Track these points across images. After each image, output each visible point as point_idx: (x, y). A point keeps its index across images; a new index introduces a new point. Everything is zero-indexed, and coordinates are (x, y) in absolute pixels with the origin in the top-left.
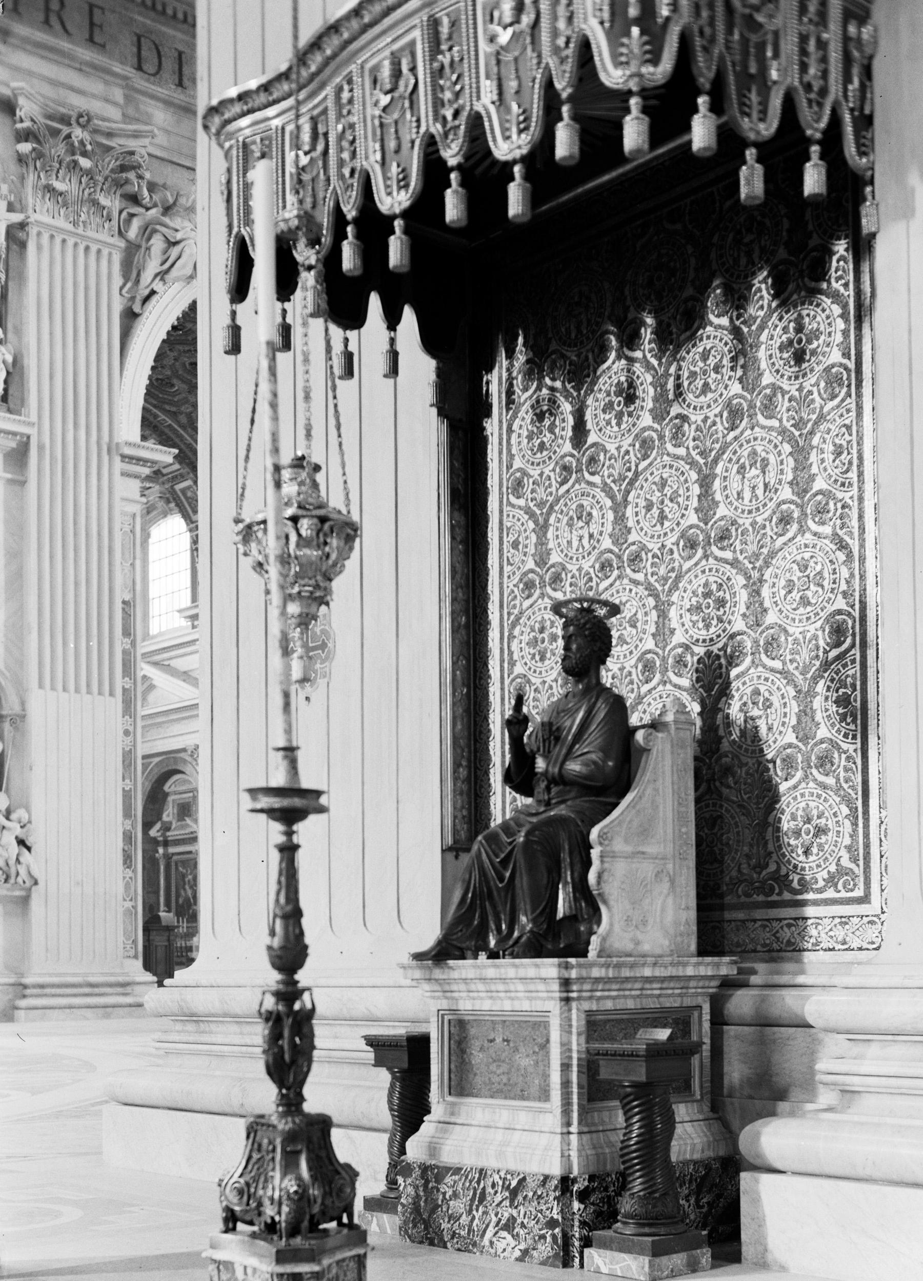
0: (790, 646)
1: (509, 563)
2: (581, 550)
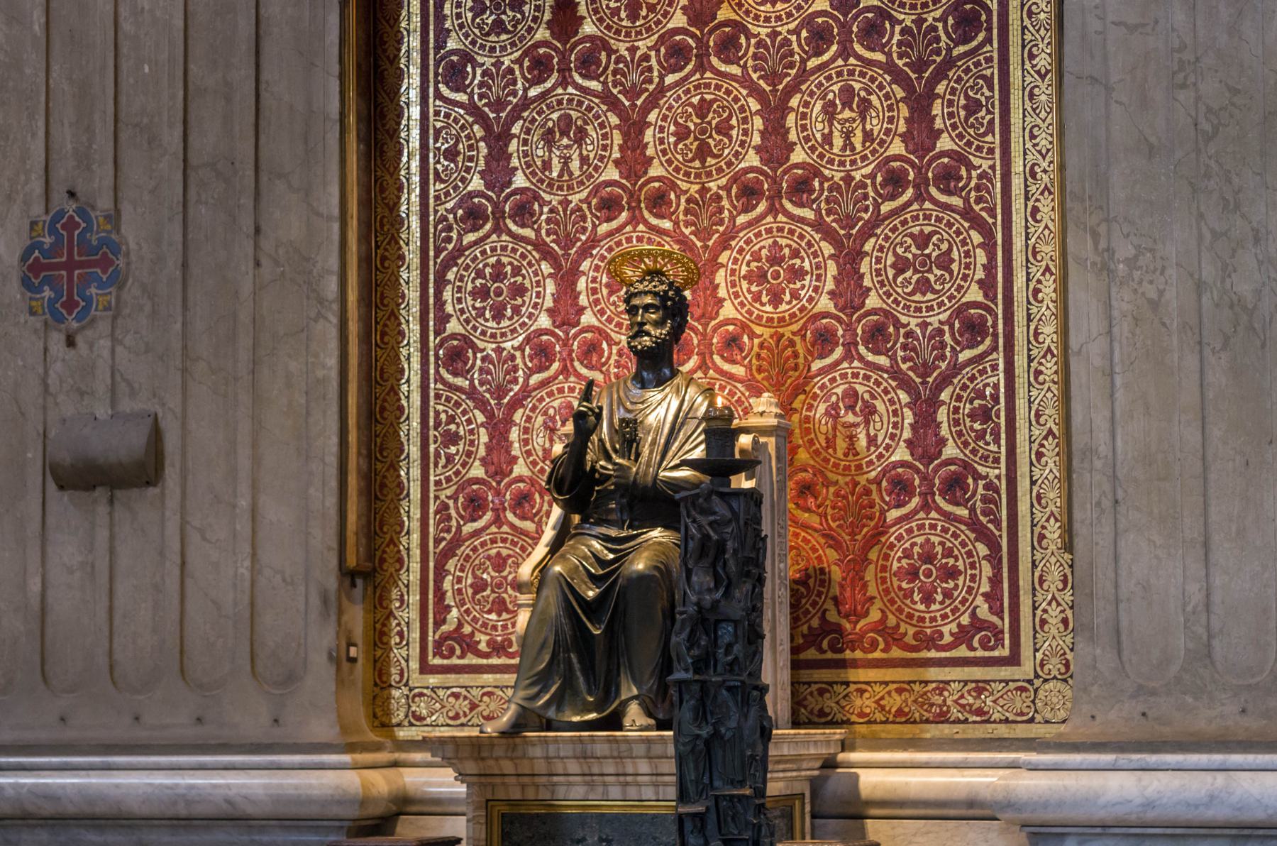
0: (902, 340)
2: (566, 177)
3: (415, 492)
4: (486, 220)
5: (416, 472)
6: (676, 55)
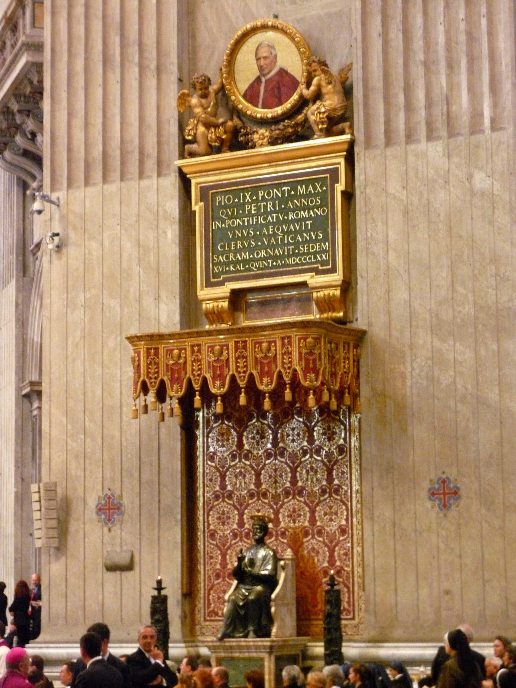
1: (207, 486)
3: (202, 571)
4: (220, 498)
5: (202, 567)
6: (269, 455)
